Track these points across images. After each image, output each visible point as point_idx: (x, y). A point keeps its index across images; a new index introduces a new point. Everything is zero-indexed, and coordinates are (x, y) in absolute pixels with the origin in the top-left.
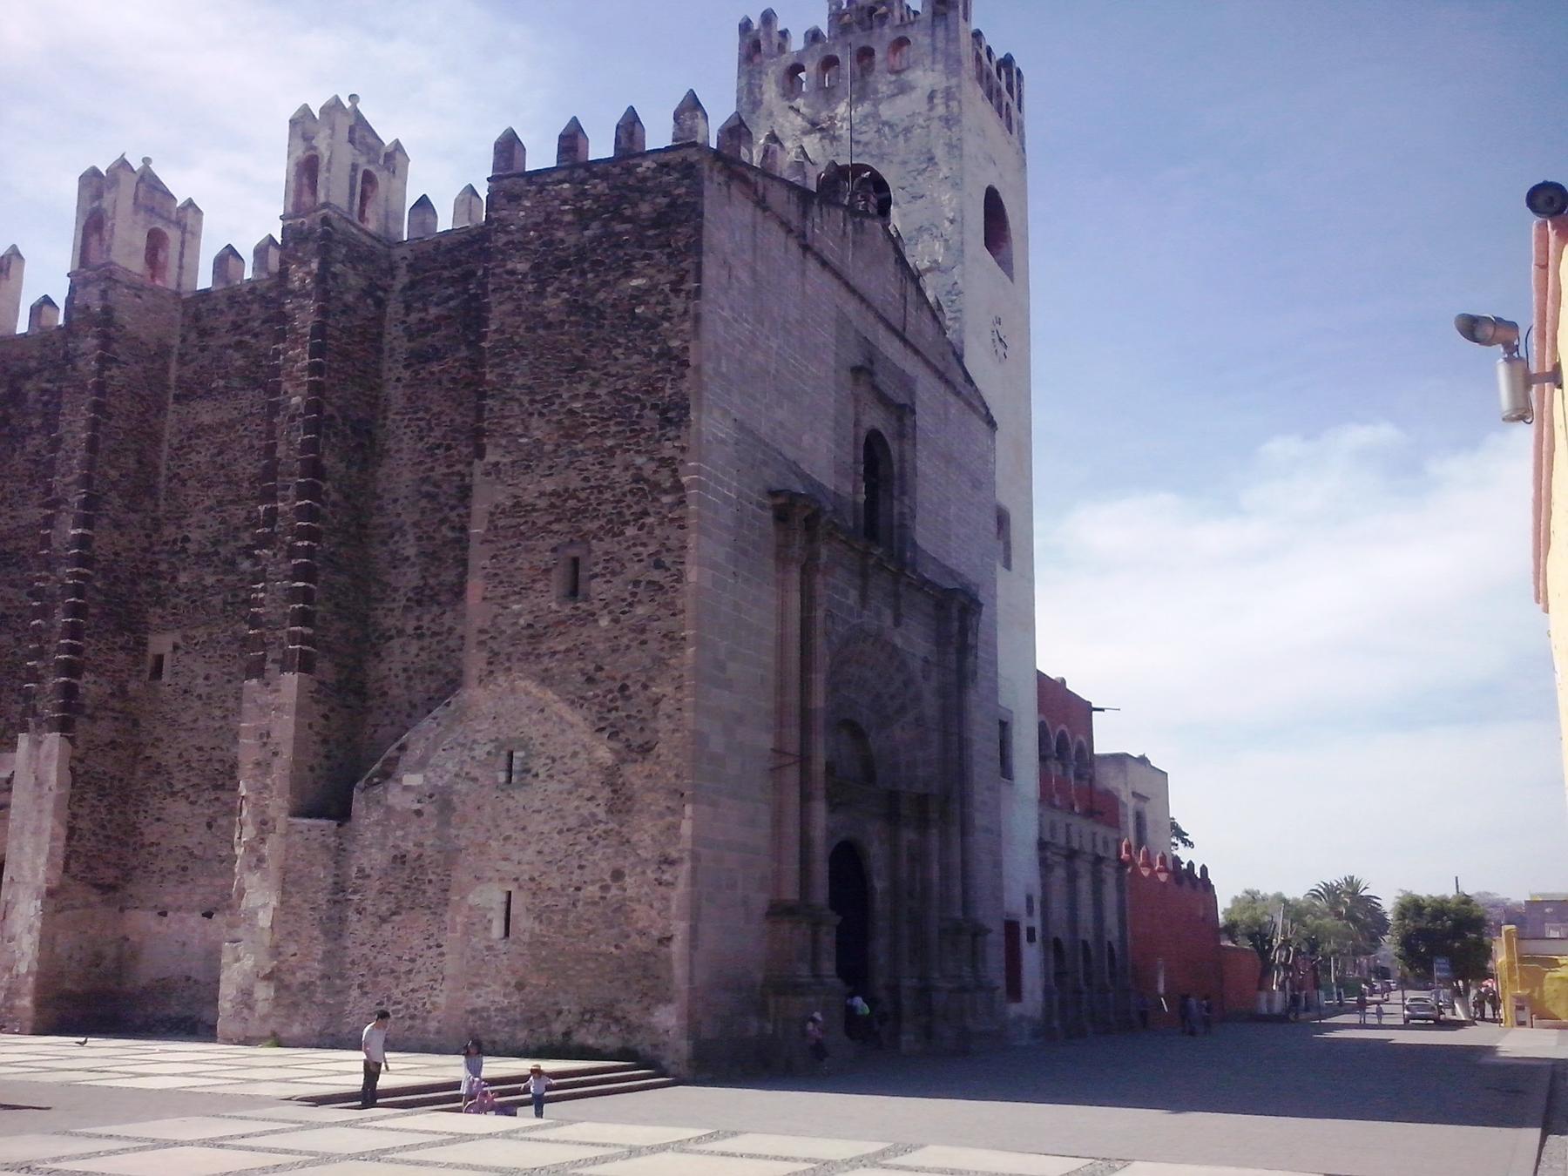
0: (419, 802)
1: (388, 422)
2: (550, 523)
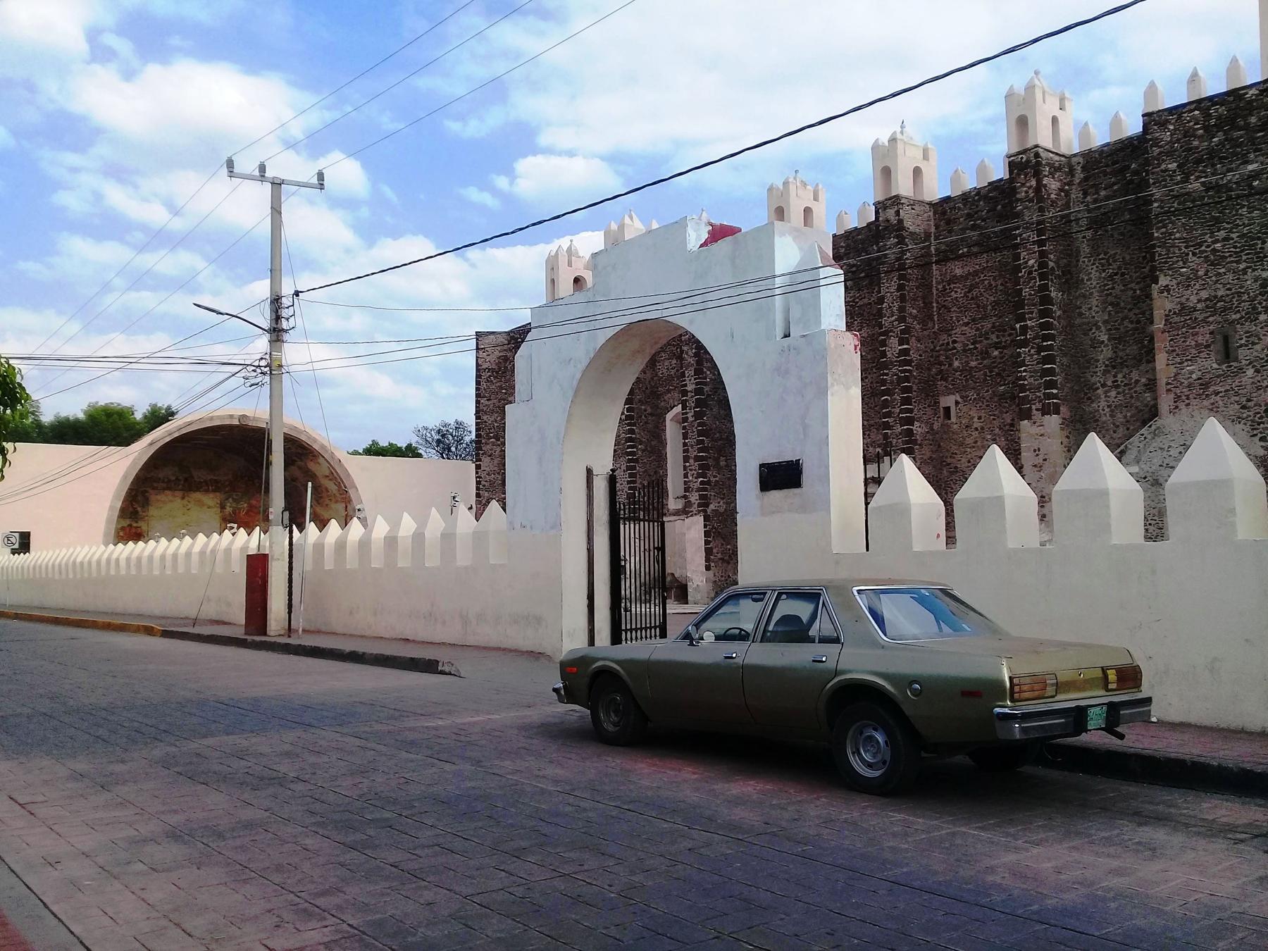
1: (1081, 263)
2: (1208, 317)
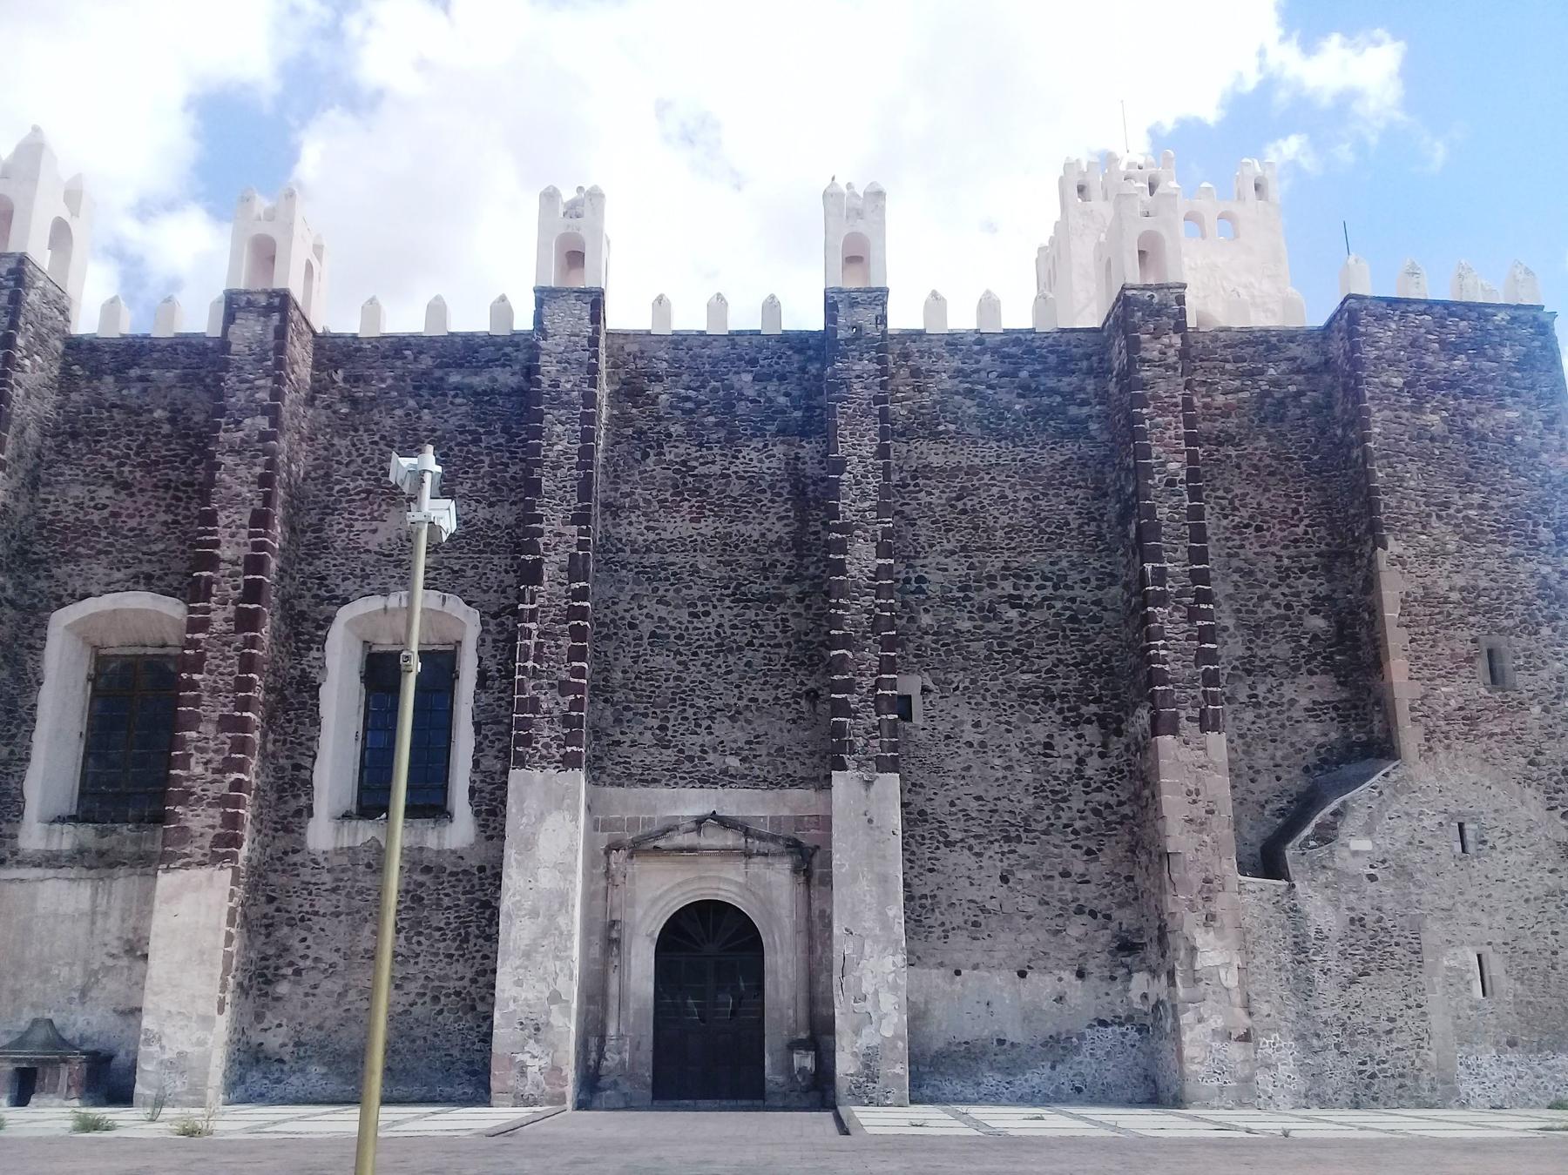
0: (1371, 867)
